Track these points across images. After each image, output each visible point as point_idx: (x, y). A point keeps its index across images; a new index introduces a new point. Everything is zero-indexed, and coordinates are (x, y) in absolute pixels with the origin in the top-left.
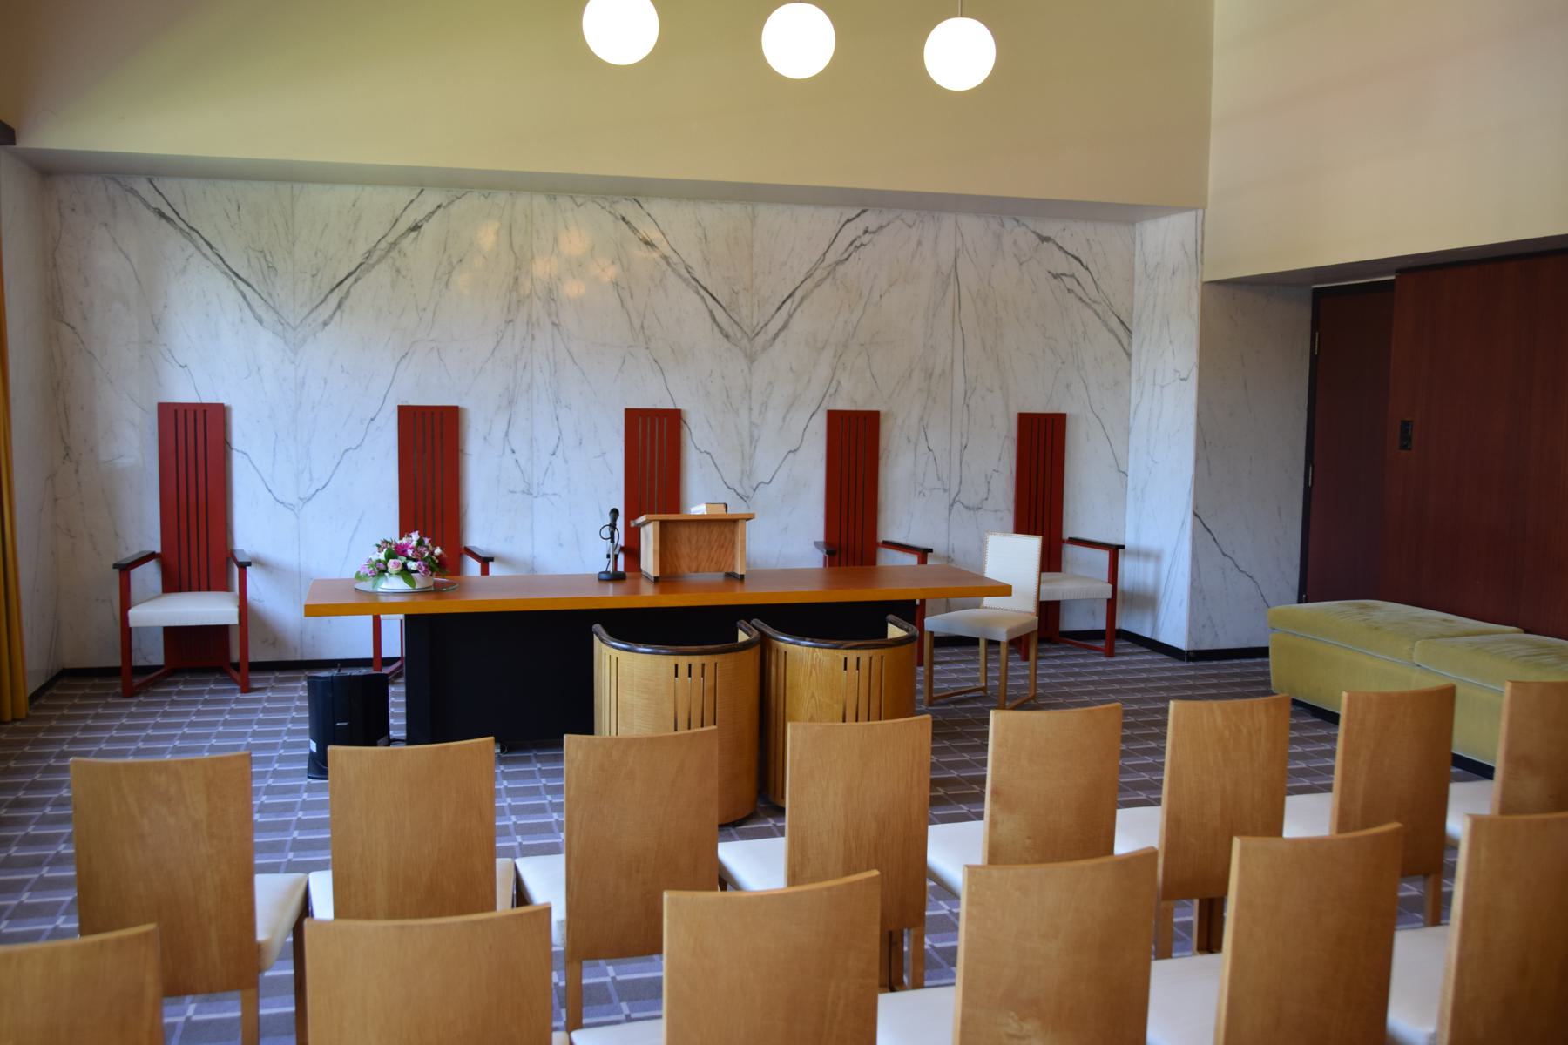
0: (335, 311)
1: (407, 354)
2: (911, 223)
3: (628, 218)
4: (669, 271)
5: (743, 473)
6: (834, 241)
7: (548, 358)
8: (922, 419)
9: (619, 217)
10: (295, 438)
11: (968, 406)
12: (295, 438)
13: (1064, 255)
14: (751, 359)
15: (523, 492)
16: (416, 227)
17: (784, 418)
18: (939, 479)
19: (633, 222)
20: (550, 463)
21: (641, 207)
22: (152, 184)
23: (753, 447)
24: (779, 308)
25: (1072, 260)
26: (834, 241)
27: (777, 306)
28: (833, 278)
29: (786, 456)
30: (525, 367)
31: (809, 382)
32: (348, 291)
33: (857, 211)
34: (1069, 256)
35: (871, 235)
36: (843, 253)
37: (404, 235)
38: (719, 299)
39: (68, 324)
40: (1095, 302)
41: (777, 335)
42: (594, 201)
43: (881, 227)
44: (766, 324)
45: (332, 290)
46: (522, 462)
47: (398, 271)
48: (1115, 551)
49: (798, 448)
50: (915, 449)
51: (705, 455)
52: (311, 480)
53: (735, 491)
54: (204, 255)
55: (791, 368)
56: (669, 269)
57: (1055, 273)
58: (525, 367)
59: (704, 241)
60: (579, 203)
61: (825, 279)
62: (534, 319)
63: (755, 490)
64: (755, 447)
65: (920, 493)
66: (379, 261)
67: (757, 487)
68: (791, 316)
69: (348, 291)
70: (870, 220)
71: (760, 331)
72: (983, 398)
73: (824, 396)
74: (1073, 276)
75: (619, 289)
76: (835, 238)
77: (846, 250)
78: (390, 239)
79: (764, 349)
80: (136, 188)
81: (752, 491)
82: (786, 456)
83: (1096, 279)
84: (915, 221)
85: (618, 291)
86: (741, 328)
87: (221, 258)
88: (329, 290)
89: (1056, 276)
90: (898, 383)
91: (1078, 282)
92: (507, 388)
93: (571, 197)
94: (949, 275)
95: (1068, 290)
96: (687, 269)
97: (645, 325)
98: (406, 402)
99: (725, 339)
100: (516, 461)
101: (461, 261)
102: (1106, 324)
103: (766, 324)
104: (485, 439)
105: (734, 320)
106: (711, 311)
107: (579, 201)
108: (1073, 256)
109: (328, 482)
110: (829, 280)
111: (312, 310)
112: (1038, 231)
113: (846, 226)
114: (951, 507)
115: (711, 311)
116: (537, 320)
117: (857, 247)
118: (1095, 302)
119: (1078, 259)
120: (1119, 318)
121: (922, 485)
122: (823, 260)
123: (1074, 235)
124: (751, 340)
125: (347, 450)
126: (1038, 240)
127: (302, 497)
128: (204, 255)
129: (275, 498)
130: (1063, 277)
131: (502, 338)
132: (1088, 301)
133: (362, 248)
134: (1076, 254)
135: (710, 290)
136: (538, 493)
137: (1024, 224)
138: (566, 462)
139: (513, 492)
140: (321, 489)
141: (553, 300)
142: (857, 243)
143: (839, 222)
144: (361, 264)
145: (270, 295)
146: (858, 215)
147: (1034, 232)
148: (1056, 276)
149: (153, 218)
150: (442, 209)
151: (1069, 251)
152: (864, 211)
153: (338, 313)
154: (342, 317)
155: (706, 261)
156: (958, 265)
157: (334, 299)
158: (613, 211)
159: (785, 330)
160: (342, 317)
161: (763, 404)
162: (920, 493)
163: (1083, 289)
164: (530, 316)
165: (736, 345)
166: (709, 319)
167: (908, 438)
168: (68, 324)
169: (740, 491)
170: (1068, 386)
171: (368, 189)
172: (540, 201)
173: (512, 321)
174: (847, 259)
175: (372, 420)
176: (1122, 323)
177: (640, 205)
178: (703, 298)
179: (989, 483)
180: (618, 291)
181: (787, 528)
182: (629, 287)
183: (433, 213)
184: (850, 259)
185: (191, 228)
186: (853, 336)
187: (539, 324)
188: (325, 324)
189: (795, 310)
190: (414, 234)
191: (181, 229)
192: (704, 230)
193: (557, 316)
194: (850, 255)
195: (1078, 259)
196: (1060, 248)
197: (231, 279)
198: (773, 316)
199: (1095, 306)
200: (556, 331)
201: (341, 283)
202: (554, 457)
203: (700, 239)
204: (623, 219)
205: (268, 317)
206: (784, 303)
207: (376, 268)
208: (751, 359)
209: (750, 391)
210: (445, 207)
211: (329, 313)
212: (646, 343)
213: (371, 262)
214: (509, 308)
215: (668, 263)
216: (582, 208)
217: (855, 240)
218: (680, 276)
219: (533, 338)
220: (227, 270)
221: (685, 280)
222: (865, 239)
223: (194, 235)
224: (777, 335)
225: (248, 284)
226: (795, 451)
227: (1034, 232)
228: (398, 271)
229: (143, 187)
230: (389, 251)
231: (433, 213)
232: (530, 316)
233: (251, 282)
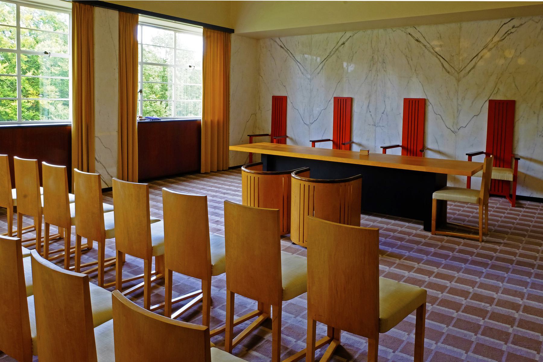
0: (321, 70)
2: (537, 21)
3: (411, 33)
4: (426, 50)
5: (454, 123)
6: (497, 33)
7: (382, 82)
9: (408, 33)
10: (310, 106)
12: (310, 106)
14: (459, 80)
15: (373, 125)
16: (344, 44)
17: (472, 103)
19: (413, 35)
20: (382, 116)
21: (416, 29)
22: (279, 39)
23: (458, 113)
24: (471, 60)
26: (497, 33)
28: (497, 48)
29: (473, 117)
30: (375, 85)
31: (484, 88)
33: (509, 20)
35: (516, 29)
36: (502, 37)
37: (340, 46)
39: (261, 76)
41: (470, 71)
42: (399, 29)
43: (521, 25)
45: (321, 64)
46: (373, 115)
47: (338, 57)
49: (479, 114)
50: (538, 117)
52: (313, 118)
53: (450, 129)
54: (290, 56)
55: (476, 83)
56: (426, 50)
58: (375, 85)
59: (440, 38)
60: (394, 30)
61: (493, 48)
62: (378, 69)
63: (459, 130)
64: (459, 113)
65: (540, 135)
66: (333, 54)
67: (460, 128)
70: (516, 22)
71: (463, 70)
73: (492, 93)
75: (408, 58)
76: (498, 31)
77: (503, 36)
78: (336, 48)
79: (464, 76)
80: (276, 40)
81: (457, 130)
82: (473, 117)
85: (407, 58)
86: (455, 69)
88: (319, 64)
90: (529, 88)
92: (369, 92)
93: (392, 29)
96: (433, 49)
97: (416, 69)
98: (339, 96)
99: (448, 73)
100: (371, 115)
101: (356, 52)
104: (361, 107)
105: (451, 66)
106: (442, 64)
107: (394, 29)
111: (315, 70)
113: (503, 26)
115: (442, 64)
116: (379, 69)
121: (541, 132)
122: (492, 41)
124: (458, 73)
127: (311, 123)
128: (290, 56)
131: (368, 76)
133: (328, 51)
135: (442, 56)
136: (378, 126)
141: (384, 63)
142: (509, 32)
143: (500, 25)
144: (328, 56)
145: (305, 66)
146: (509, 21)
149: (279, 48)
150: (351, 37)
152: (512, 19)
153: (322, 70)
154: (323, 71)
158: (406, 32)
159: (474, 69)
160: (323, 71)
161: (463, 97)
162: (540, 135)
164: (377, 68)
165: (452, 75)
167: (534, 112)
168: (261, 76)
169: (453, 130)
172: (381, 31)
173: (370, 71)
174: (504, 39)
175: (330, 101)
178: (439, 59)
180: (407, 58)
181: (472, 145)
182: (411, 57)
183: (348, 39)
184: (505, 39)
185: (288, 50)
186: (506, 70)
187: (380, 71)
188: (318, 73)
189: (478, 61)
190: (343, 46)
191: (285, 50)
192: (440, 35)
193: (386, 68)
194: (505, 38)
197: (296, 62)
200: (385, 72)
201: (323, 61)
202: (383, 114)
203: (438, 38)
204: (409, 34)
207: (332, 56)
208: (459, 80)
209: (458, 92)
210: (352, 37)
212: (417, 76)
213: (331, 55)
214: (370, 66)
215: (426, 47)
216: (395, 32)
217: (508, 31)
218: (430, 51)
219: (378, 75)
220: (295, 60)
221: (432, 53)
222: (513, 30)
223: (288, 51)
224: (470, 71)
225: (300, 64)
226: (477, 115)
228: (338, 57)
229: (278, 40)
230: (335, 51)
231: (348, 39)
232: (377, 68)
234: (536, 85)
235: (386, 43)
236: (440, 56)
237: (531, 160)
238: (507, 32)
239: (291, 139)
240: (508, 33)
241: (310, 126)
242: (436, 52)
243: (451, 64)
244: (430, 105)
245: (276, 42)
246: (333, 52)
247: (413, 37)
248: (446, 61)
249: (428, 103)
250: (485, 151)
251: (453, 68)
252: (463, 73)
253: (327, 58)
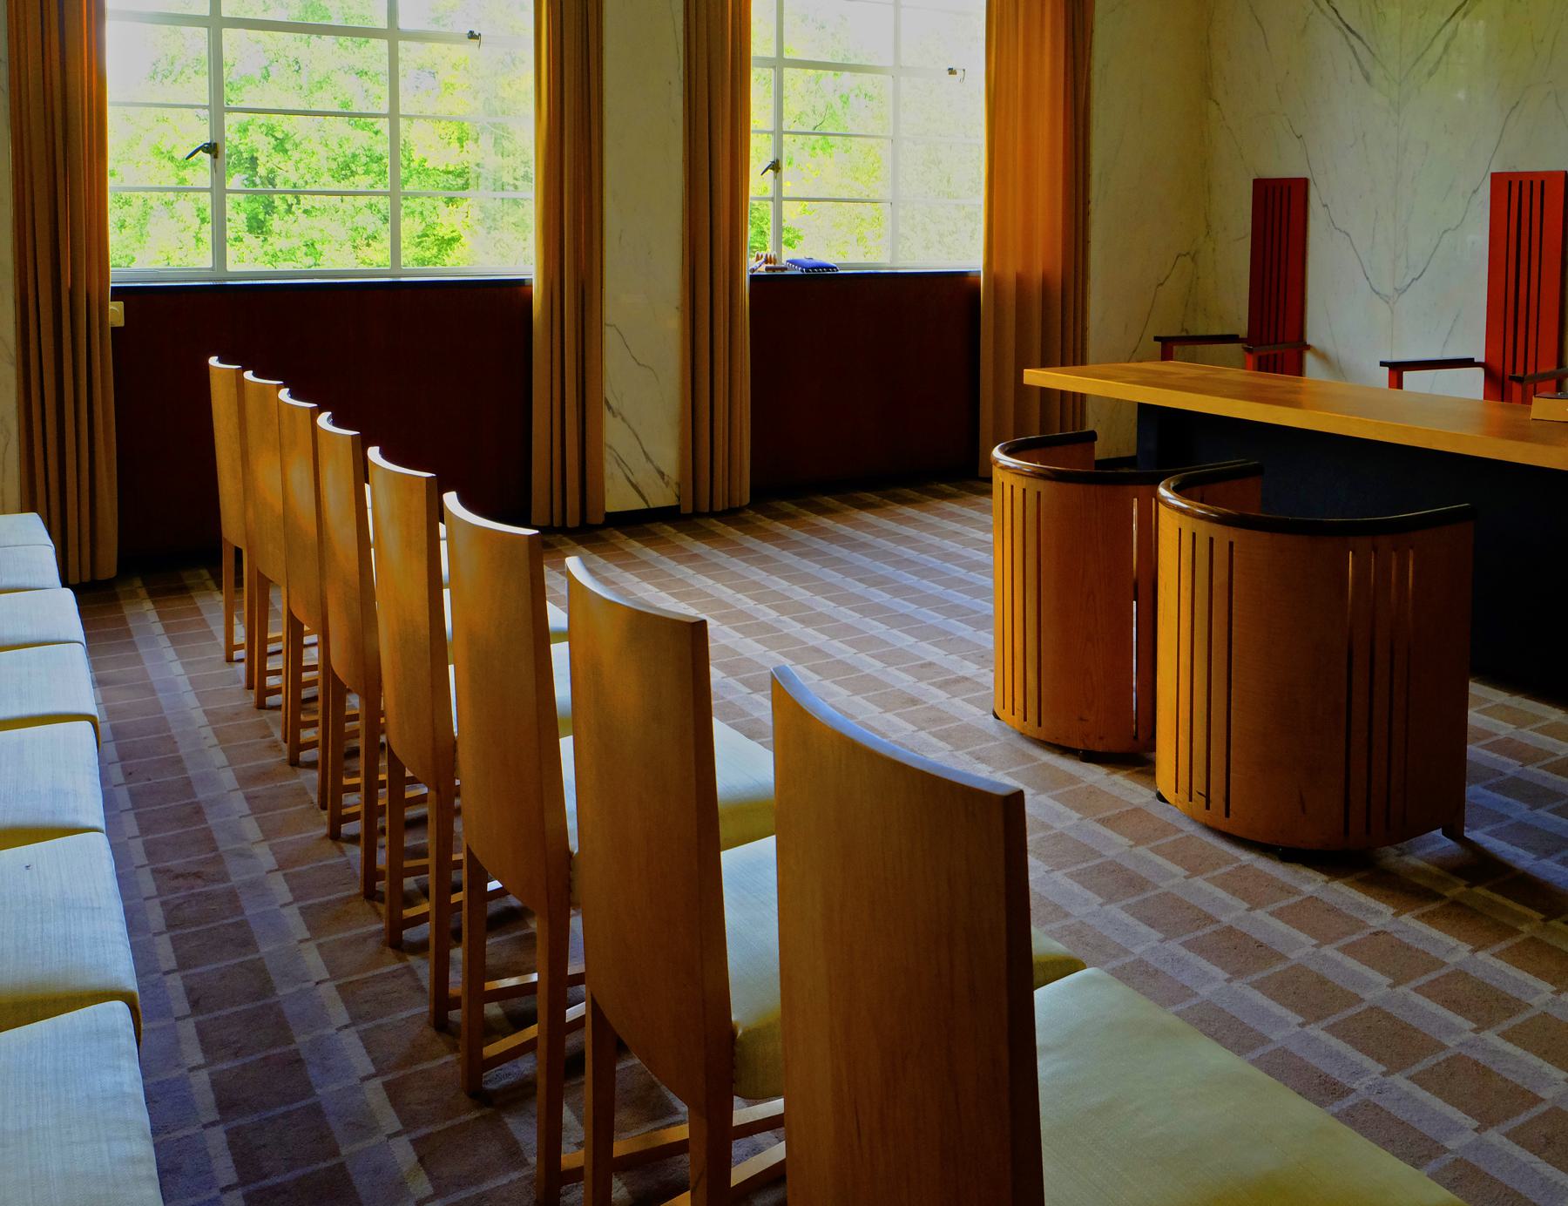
1: (1518, 103)
87: (1336, 11)
98: (1515, 167)
109: (1424, 271)
111: (1418, 59)
125: (1445, 231)
127: (1398, 288)
129: (1371, 287)
140: (1417, 279)
175: (1475, 192)
188: (1430, 74)
197: (1344, 33)
225: (1359, 38)
233: (1362, 33)
239: (1323, 357)
241: (1394, 303)
253: (1466, 5)
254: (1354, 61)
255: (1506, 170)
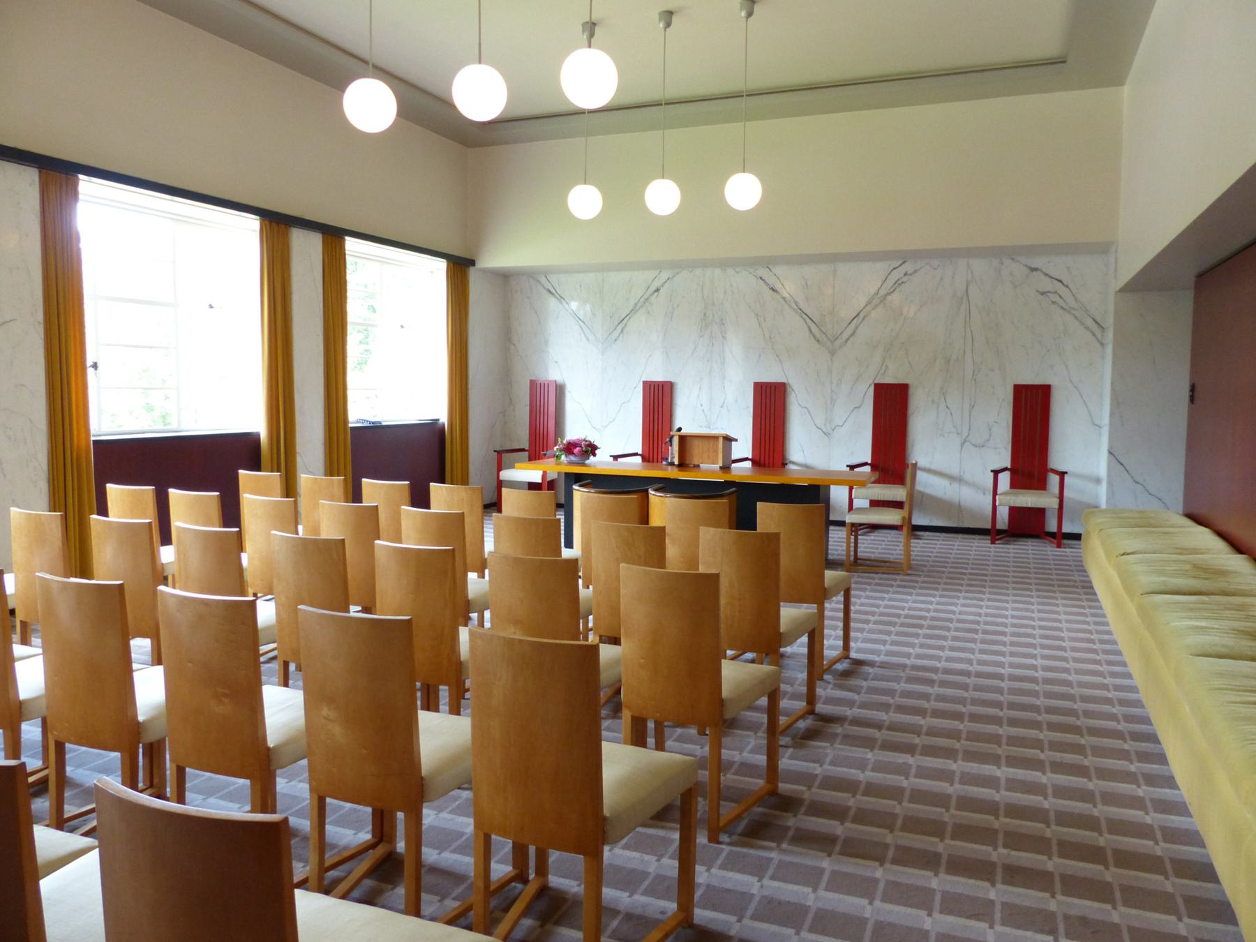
3: (763, 278)
8: (942, 388)
11: (975, 380)
13: (1049, 279)
14: (833, 353)
15: (706, 427)
16: (658, 290)
18: (954, 426)
24: (850, 324)
25: (1056, 281)
27: (849, 322)
32: (626, 324)
33: (901, 262)
34: (1053, 280)
35: (910, 277)
38: (814, 320)
40: (1074, 309)
41: (848, 339)
43: (916, 271)
44: (841, 333)
47: (649, 313)
48: (1062, 475)
49: (861, 404)
51: (804, 409)
56: (786, 304)
57: (1040, 290)
62: (713, 335)
63: (833, 430)
66: (639, 309)
68: (857, 328)
69: (626, 324)
70: (908, 267)
72: (986, 376)
73: (878, 373)
74: (1056, 292)
78: (646, 297)
79: (841, 347)
81: (832, 431)
83: (1074, 293)
84: (939, 266)
88: (617, 323)
89: (1043, 294)
91: (1060, 296)
94: (962, 298)
95: (1053, 302)
97: (772, 336)
102: (1082, 323)
103: (841, 333)
106: (809, 327)
107: (738, 270)
108: (1057, 279)
110: (882, 305)
112: (1029, 264)
114: (962, 444)
115: (809, 327)
117: (899, 285)
118: (1074, 309)
119: (1060, 281)
120: (1094, 320)
123: (1056, 265)
126: (1029, 270)
130: (1048, 294)
132: (1069, 309)
133: (632, 302)
134: (1059, 278)
135: (808, 314)
137: (1018, 261)
138: (728, 411)
139: (701, 427)
141: (723, 324)
142: (899, 282)
144: (632, 310)
146: (901, 265)
147: (1026, 266)
148: (1043, 294)
149: (547, 293)
151: (1053, 276)
152: (905, 262)
154: (623, 337)
155: (807, 299)
156: (969, 291)
157: (619, 328)
163: (1064, 301)
164: (711, 332)
166: (807, 330)
170: (1052, 367)
171: (636, 273)
172: (718, 271)
176: (1096, 322)
177: (770, 269)
178: (804, 320)
179: (990, 430)
183: (665, 282)
185: (561, 297)
188: (616, 340)
190: (656, 294)
195: (1060, 281)
196: (1046, 275)
198: (846, 328)
199: (1074, 312)
201: (623, 320)
204: (761, 278)
205: (591, 337)
206: (852, 320)
208: (833, 353)
211: (618, 334)
217: (899, 280)
218: (791, 307)
221: (794, 310)
222: (905, 279)
224: (848, 339)
225: (584, 323)
227: (1026, 266)
228: (649, 313)
229: (543, 280)
230: (644, 303)
231: (665, 282)
232: (711, 332)
234: (935, 361)
235: (725, 292)
236: (807, 315)
237: (929, 471)
238: (895, 284)
240: (899, 283)
242: (801, 310)
243: (823, 329)
244: (793, 393)
245: (539, 282)
246: (640, 304)
247: (767, 284)
248: (814, 323)
249: (789, 390)
250: (869, 462)
251: (824, 333)
252: (838, 343)
254: (582, 332)
255: (648, 380)
